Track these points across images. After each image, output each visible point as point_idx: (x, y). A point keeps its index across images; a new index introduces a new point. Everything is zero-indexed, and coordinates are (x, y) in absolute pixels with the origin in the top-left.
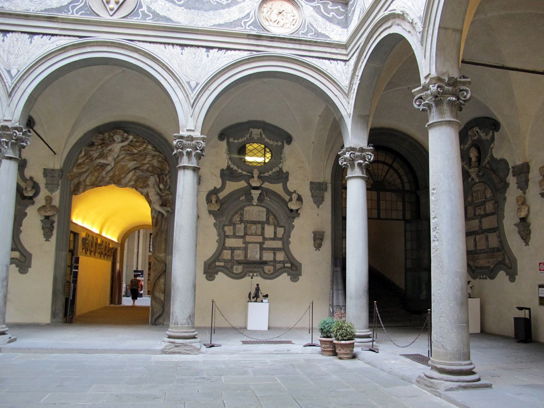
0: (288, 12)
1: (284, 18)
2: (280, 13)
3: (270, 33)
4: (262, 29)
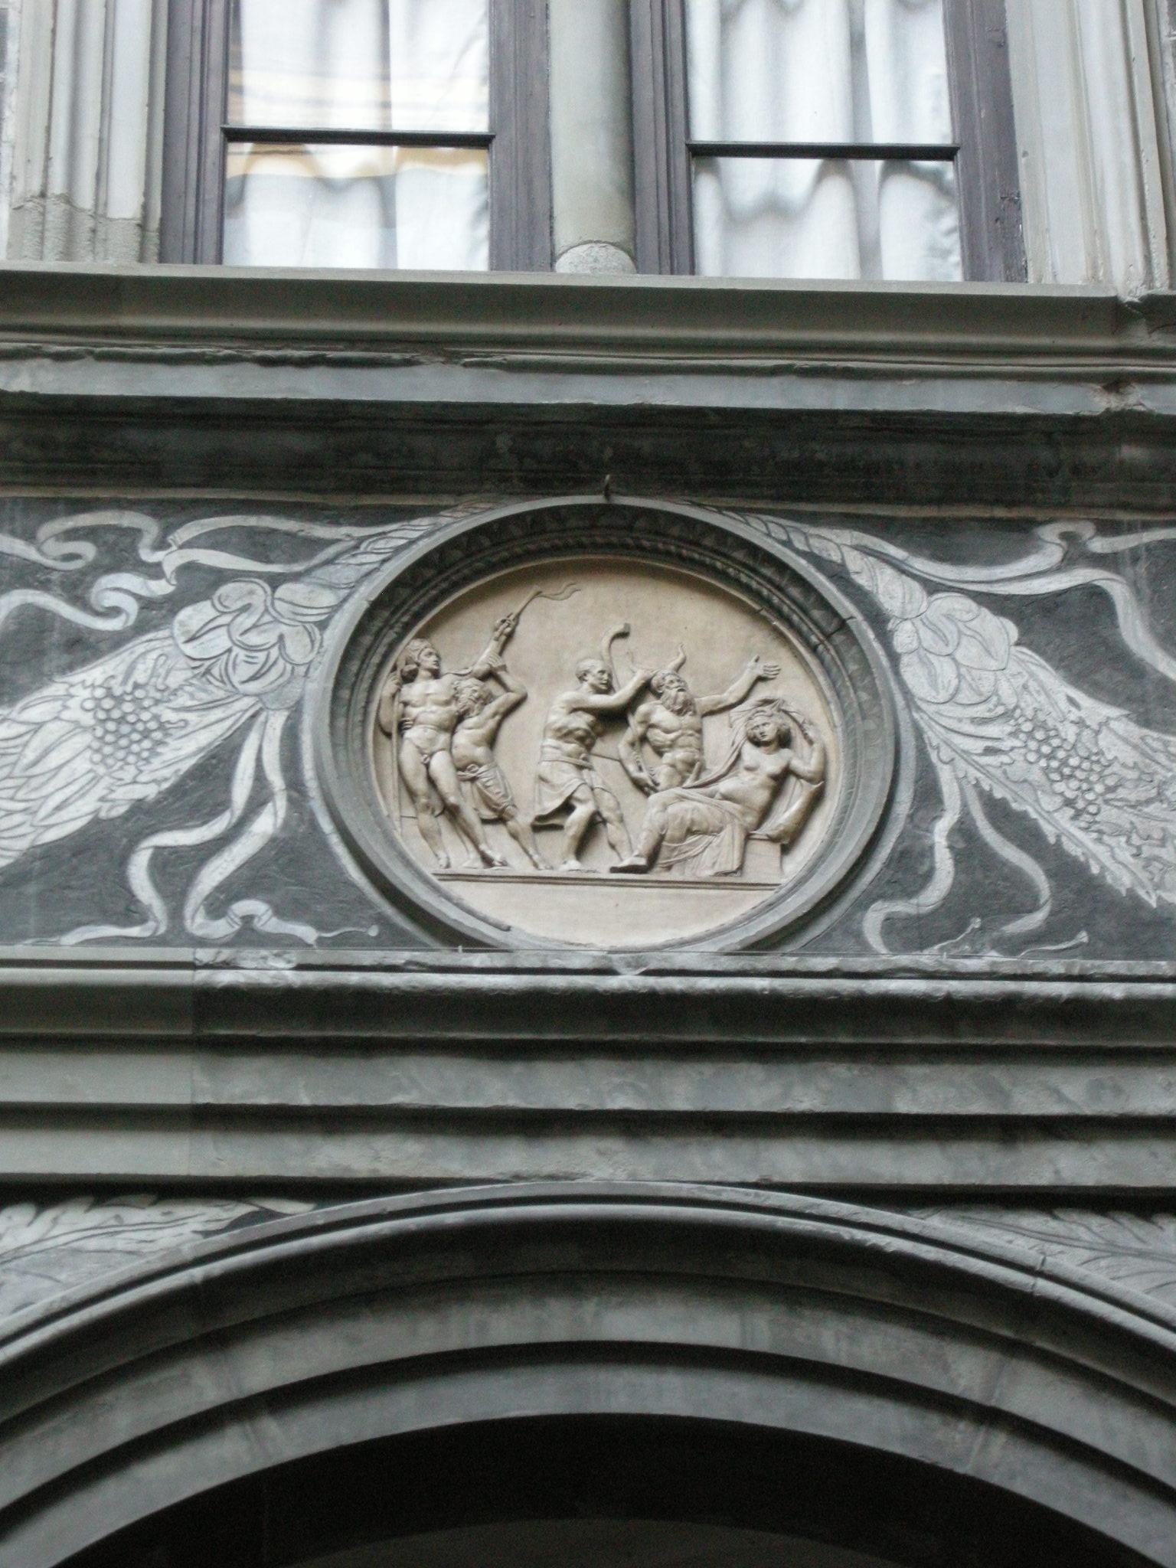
0: (705, 700)
1: (661, 770)
2: (611, 720)
3: (478, 960)
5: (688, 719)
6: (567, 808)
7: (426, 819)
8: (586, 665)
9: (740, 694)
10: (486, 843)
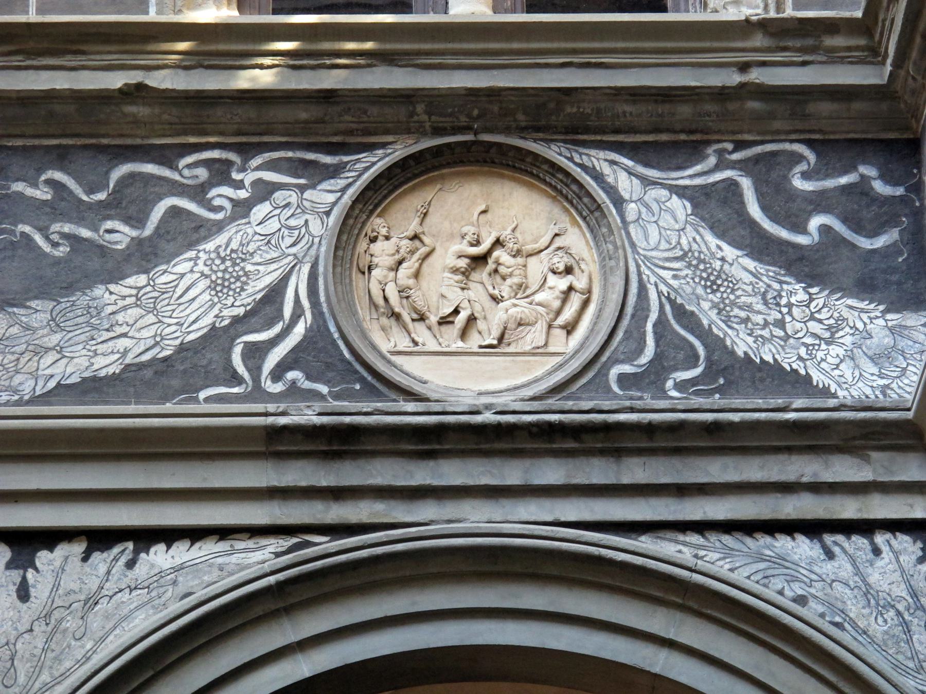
0: (529, 247)
1: (505, 290)
2: (480, 260)
4: (362, 380)
5: (520, 260)
6: (456, 312)
7: (384, 321)
8: (465, 229)
9: (547, 244)
10: (415, 333)
